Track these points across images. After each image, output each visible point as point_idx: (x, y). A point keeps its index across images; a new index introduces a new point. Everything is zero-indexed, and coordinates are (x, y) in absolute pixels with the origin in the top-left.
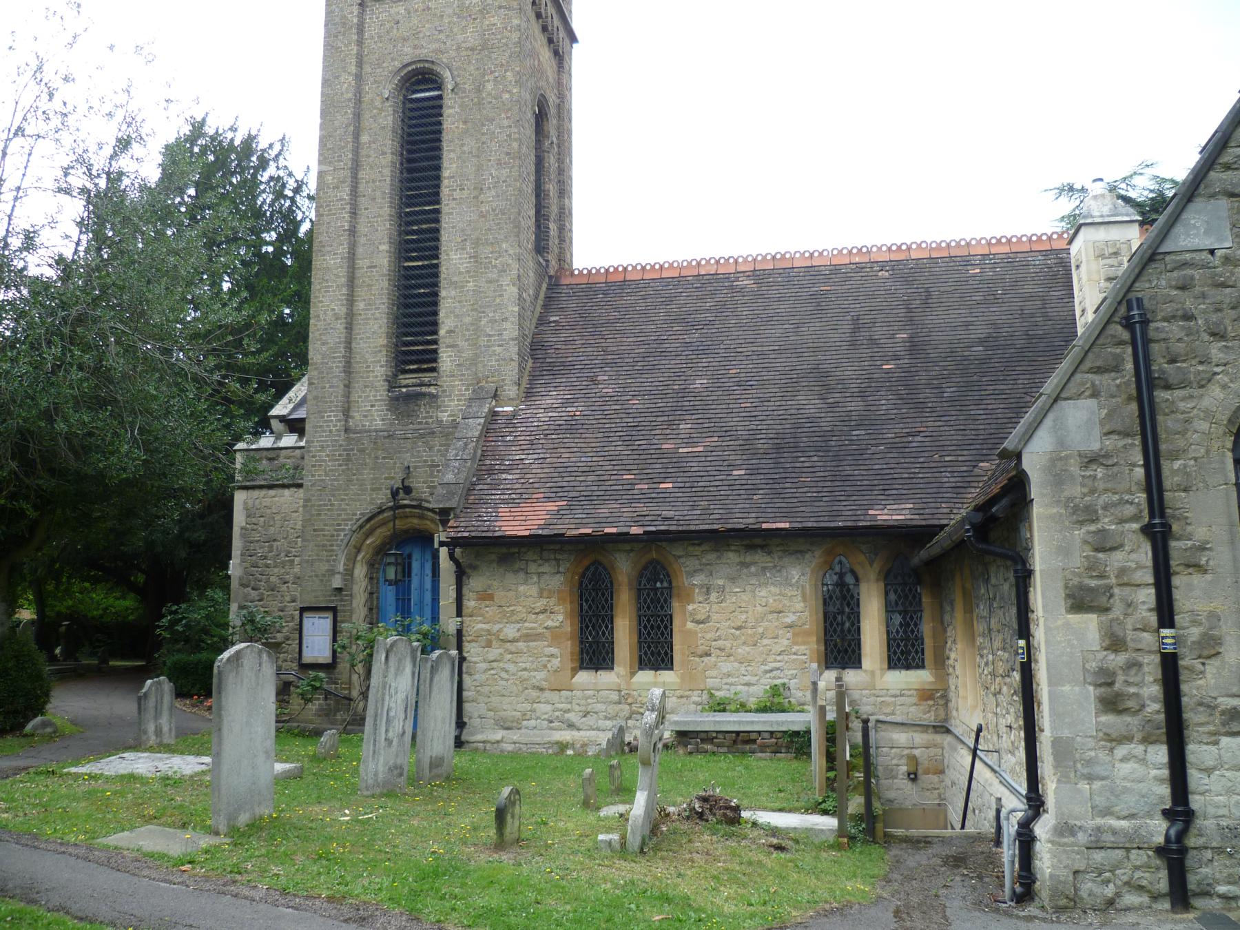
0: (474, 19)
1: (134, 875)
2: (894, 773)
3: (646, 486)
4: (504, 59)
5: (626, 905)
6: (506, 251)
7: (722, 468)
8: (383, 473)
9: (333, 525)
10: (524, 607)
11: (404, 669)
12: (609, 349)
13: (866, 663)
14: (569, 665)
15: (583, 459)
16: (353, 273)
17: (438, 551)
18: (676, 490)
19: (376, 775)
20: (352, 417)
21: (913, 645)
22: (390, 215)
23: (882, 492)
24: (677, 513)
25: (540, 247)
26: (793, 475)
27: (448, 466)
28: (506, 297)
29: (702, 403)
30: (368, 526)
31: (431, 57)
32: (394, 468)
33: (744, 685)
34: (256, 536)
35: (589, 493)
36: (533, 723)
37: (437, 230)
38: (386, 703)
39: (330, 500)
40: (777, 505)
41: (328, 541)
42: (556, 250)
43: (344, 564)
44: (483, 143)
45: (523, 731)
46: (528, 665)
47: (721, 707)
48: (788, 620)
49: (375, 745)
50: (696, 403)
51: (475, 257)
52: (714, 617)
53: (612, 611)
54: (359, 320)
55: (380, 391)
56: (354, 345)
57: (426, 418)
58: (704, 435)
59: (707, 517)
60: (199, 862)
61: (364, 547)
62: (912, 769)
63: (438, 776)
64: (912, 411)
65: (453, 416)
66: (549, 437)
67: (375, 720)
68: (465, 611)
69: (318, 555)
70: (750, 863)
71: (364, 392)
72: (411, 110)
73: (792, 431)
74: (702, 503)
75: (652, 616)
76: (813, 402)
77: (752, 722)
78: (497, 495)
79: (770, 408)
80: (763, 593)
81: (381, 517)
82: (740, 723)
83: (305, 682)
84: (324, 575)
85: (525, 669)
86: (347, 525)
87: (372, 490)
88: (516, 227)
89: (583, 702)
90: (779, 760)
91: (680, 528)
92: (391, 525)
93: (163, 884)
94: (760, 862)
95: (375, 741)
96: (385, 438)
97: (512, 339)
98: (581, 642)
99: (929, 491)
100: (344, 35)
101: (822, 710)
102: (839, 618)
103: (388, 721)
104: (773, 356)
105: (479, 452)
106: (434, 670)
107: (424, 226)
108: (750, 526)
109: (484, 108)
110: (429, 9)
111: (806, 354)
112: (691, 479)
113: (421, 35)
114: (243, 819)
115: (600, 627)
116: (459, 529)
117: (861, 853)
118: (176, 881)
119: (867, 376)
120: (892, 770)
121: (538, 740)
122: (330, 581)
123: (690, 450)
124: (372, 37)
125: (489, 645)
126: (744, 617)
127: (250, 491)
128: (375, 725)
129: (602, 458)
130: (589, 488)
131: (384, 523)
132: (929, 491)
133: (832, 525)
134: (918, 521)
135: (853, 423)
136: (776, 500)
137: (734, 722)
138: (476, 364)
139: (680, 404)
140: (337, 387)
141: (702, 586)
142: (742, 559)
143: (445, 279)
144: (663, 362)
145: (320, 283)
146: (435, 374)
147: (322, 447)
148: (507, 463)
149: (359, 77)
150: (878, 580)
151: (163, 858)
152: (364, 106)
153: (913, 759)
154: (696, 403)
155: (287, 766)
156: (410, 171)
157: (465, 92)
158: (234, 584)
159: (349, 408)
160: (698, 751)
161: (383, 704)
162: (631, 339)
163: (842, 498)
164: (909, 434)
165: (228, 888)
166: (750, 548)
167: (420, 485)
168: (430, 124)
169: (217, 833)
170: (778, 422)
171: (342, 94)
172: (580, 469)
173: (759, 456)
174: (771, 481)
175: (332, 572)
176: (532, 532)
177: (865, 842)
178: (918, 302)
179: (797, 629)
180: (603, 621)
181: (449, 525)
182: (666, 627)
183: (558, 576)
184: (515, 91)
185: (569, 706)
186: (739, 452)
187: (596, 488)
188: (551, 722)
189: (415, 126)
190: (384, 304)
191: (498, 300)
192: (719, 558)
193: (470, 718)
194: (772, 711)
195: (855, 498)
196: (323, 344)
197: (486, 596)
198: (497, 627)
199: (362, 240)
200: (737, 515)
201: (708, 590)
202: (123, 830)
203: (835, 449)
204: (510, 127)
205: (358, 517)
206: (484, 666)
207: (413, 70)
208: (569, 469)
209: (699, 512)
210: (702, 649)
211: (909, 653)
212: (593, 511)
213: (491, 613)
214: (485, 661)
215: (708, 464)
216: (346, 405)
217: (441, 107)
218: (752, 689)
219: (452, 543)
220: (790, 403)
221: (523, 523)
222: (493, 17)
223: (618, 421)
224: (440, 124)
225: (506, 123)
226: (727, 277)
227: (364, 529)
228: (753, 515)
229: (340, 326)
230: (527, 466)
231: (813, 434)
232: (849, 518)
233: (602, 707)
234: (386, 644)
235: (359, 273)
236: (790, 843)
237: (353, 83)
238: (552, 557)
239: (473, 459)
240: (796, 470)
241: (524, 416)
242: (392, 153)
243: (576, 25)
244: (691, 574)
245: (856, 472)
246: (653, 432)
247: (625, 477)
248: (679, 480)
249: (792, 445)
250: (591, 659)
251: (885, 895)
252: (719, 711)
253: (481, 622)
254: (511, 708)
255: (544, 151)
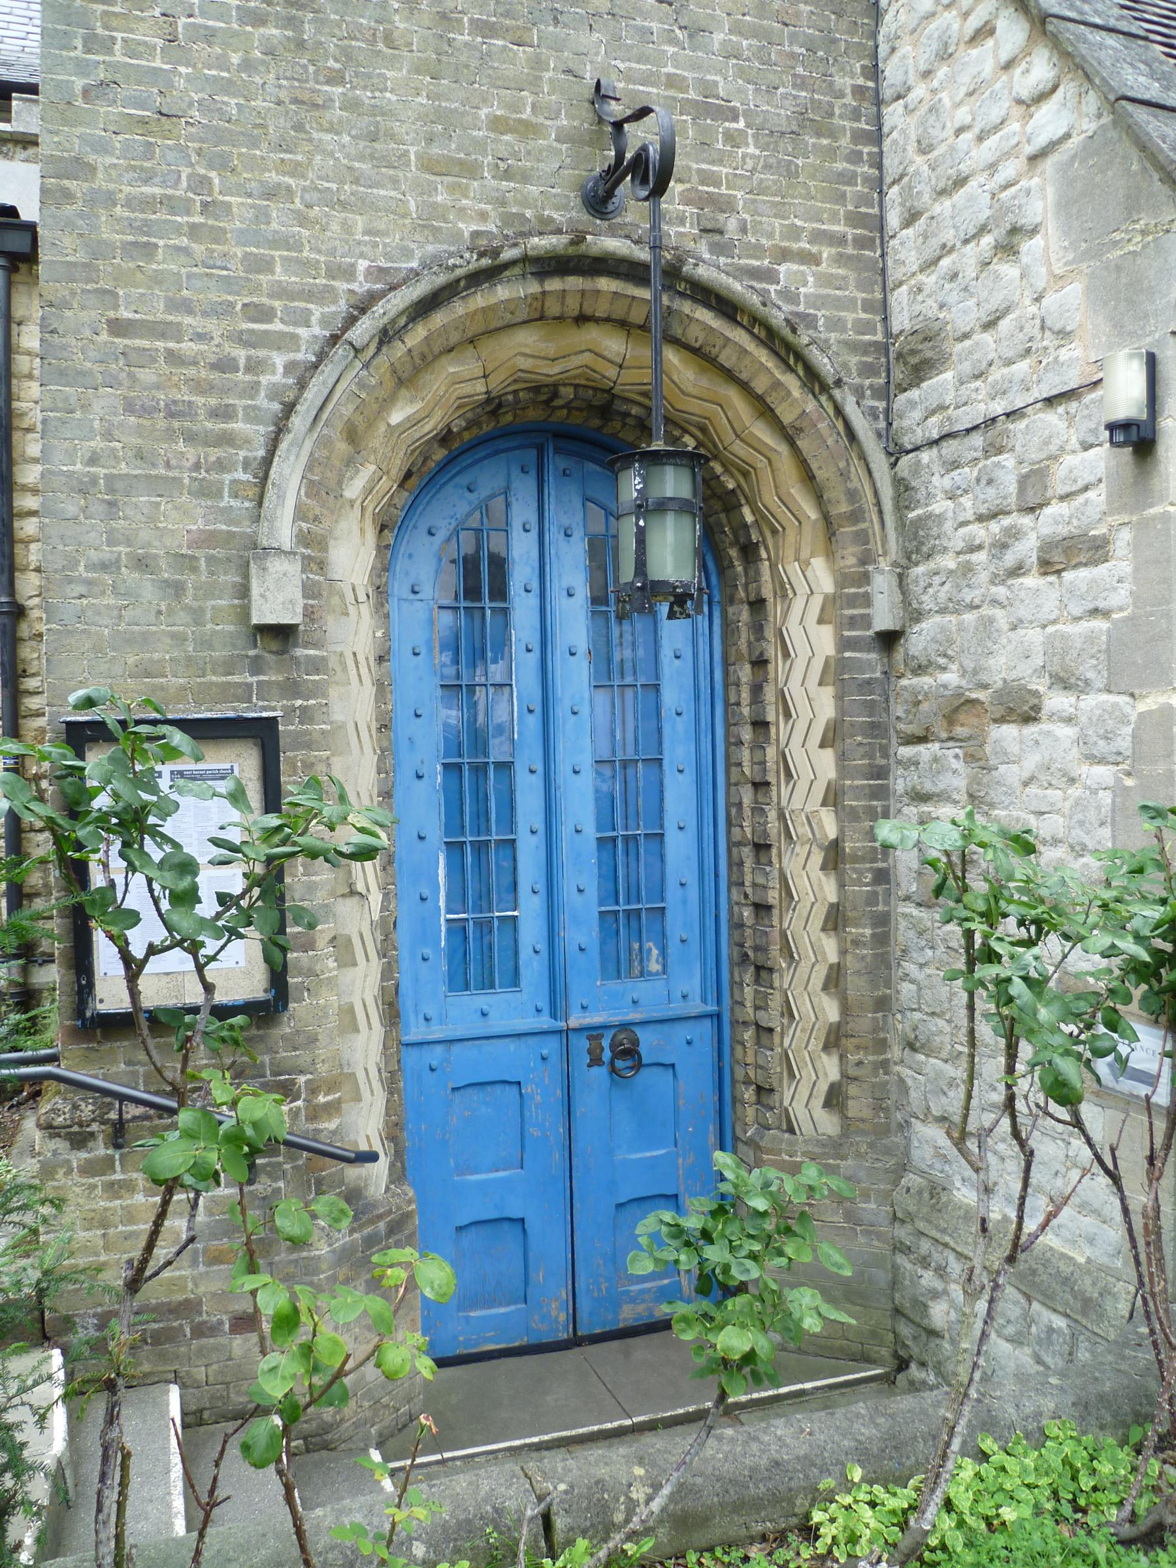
30: (418, 334)
32: (534, 83)
41: (200, 387)
61: (377, 440)
81: (480, 299)
84: (187, 563)
205: (361, 286)
227: (398, 350)
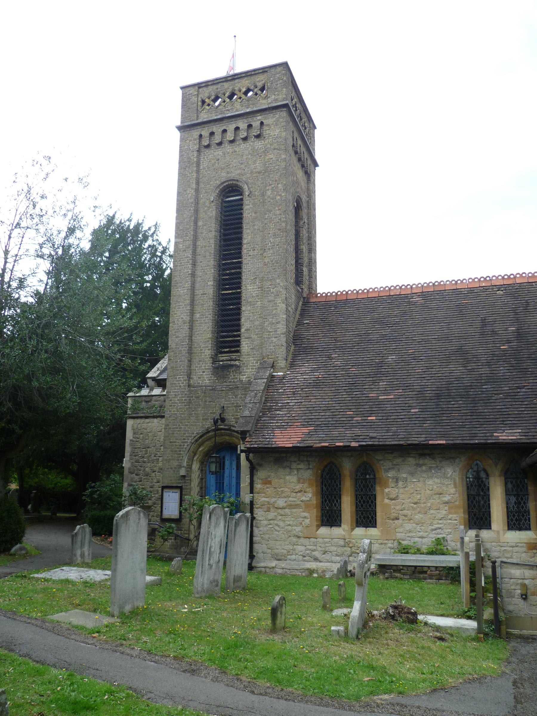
0: (260, 156)
1: (67, 638)
2: (512, 594)
3: (360, 419)
4: (277, 177)
5: (348, 670)
6: (279, 284)
7: (404, 408)
8: (210, 410)
9: (180, 439)
10: (289, 488)
11: (220, 523)
12: (338, 339)
13: (494, 526)
14: (315, 523)
15: (323, 403)
16: (193, 297)
17: (240, 455)
18: (378, 421)
19: (203, 585)
20: (192, 379)
21: (523, 516)
22: (214, 265)
23: (502, 423)
24: (378, 434)
25: (298, 281)
26: (448, 412)
27: (246, 406)
28: (279, 310)
29: (393, 370)
31: (237, 178)
33: (419, 537)
34: (138, 445)
35: (327, 423)
36: (293, 557)
37: (240, 273)
38: (209, 543)
39: (179, 425)
40: (438, 430)
41: (178, 448)
42: (307, 283)
43: (187, 462)
44: (266, 224)
45: (288, 561)
46: (291, 523)
47: (405, 551)
48: (446, 499)
49: (202, 567)
50: (389, 370)
51: (261, 288)
52: (401, 496)
53: (340, 491)
54: (197, 324)
55: (208, 364)
56: (193, 338)
57: (233, 379)
58: (394, 389)
59: (396, 437)
60: (103, 632)
61: (198, 452)
62: (524, 592)
63: (239, 587)
64: (519, 373)
65: (249, 377)
66: (304, 390)
67: (203, 553)
68: (255, 490)
69: (172, 456)
70: (423, 648)
71: (199, 364)
72: (226, 207)
73: (447, 386)
74: (393, 429)
75: (364, 495)
76: (459, 369)
77: (424, 561)
78: (274, 423)
79: (433, 373)
80: (430, 482)
82: (417, 561)
83: (164, 529)
84: (175, 468)
85: (289, 525)
86: (189, 440)
87: (203, 420)
88: (284, 270)
89: (323, 545)
90: (441, 584)
91: (380, 443)
92: (214, 439)
93: (82, 644)
94: (429, 648)
95: (202, 565)
96: (210, 390)
97: (282, 334)
98: (322, 510)
99: (531, 421)
100: (189, 168)
101: (467, 555)
102: (477, 498)
103: (210, 554)
104: (434, 342)
105: (264, 398)
106: (237, 525)
107: (233, 271)
108: (422, 443)
109: (266, 205)
110: (235, 151)
111: (454, 341)
112: (387, 415)
113: (231, 166)
114: (128, 608)
115: (333, 501)
116: (252, 443)
117: (492, 644)
118: (90, 643)
119: (491, 353)
120: (511, 592)
121: (297, 567)
122: (179, 471)
123: (386, 397)
124: (204, 168)
125: (268, 510)
126: (419, 497)
127: (135, 420)
128: (203, 556)
129: (334, 402)
130: (327, 420)
131: (209, 439)
132: (531, 421)
133: (472, 442)
134: (524, 440)
135: (483, 381)
136: (437, 427)
137: (414, 560)
138: (262, 348)
139: (379, 370)
140: (184, 361)
141: (393, 478)
142: (417, 462)
143: (245, 300)
144: (370, 346)
145: (175, 304)
146: (239, 354)
147: (176, 395)
148: (280, 405)
149: (197, 190)
150: (500, 476)
151: (83, 629)
152: (200, 206)
153: (524, 586)
154: (389, 370)
155: (153, 578)
156: (225, 240)
157: (255, 196)
158: (126, 472)
159: (190, 373)
160: (392, 577)
161: (207, 544)
162: (351, 333)
163: (478, 426)
164: (518, 388)
165: (118, 648)
166: (422, 455)
167: (230, 417)
168: (236, 215)
169: (113, 616)
170: (438, 381)
171: (188, 200)
172: (322, 409)
173: (427, 401)
174: (434, 416)
175: (180, 467)
176: (294, 445)
177: (494, 637)
178: (521, 308)
179: (451, 505)
180: (335, 497)
181: (246, 440)
182: (372, 502)
183: (309, 470)
184: (283, 194)
185: (315, 548)
186: (415, 399)
187: (330, 420)
188: (304, 557)
189: (228, 216)
190: (210, 314)
191: (274, 312)
192: (403, 461)
193: (257, 553)
194: (437, 554)
195: (485, 426)
196: (177, 337)
197: (266, 482)
198: (274, 500)
199: (199, 279)
200: (414, 436)
201: (397, 480)
202: (62, 612)
203: (473, 396)
204: (281, 214)
206: (266, 522)
207: (227, 185)
208: (315, 409)
209: (391, 434)
210: (394, 515)
211: (521, 520)
212: (329, 433)
213: (270, 492)
214: (266, 519)
215: (397, 405)
216: (189, 372)
217: (242, 205)
218: (425, 540)
219: (248, 451)
220: (445, 369)
221: (289, 440)
222: (271, 154)
223: (343, 380)
224: (242, 214)
225: (278, 212)
226: (406, 296)
227: (198, 442)
228: (424, 436)
229: (186, 327)
230: (291, 407)
231: (459, 388)
232: (482, 438)
233: (333, 548)
234: (210, 509)
235: (196, 298)
236: (448, 636)
237: (194, 194)
238: (306, 459)
239: (260, 402)
240: (449, 409)
241: (289, 378)
242: (215, 231)
243: (318, 157)
244: (387, 471)
245: (486, 411)
246: (364, 387)
247: (348, 413)
248: (379, 415)
249: (446, 394)
250: (328, 520)
251: (507, 671)
252: (404, 553)
253: (264, 497)
254: (281, 548)
255: (300, 227)
